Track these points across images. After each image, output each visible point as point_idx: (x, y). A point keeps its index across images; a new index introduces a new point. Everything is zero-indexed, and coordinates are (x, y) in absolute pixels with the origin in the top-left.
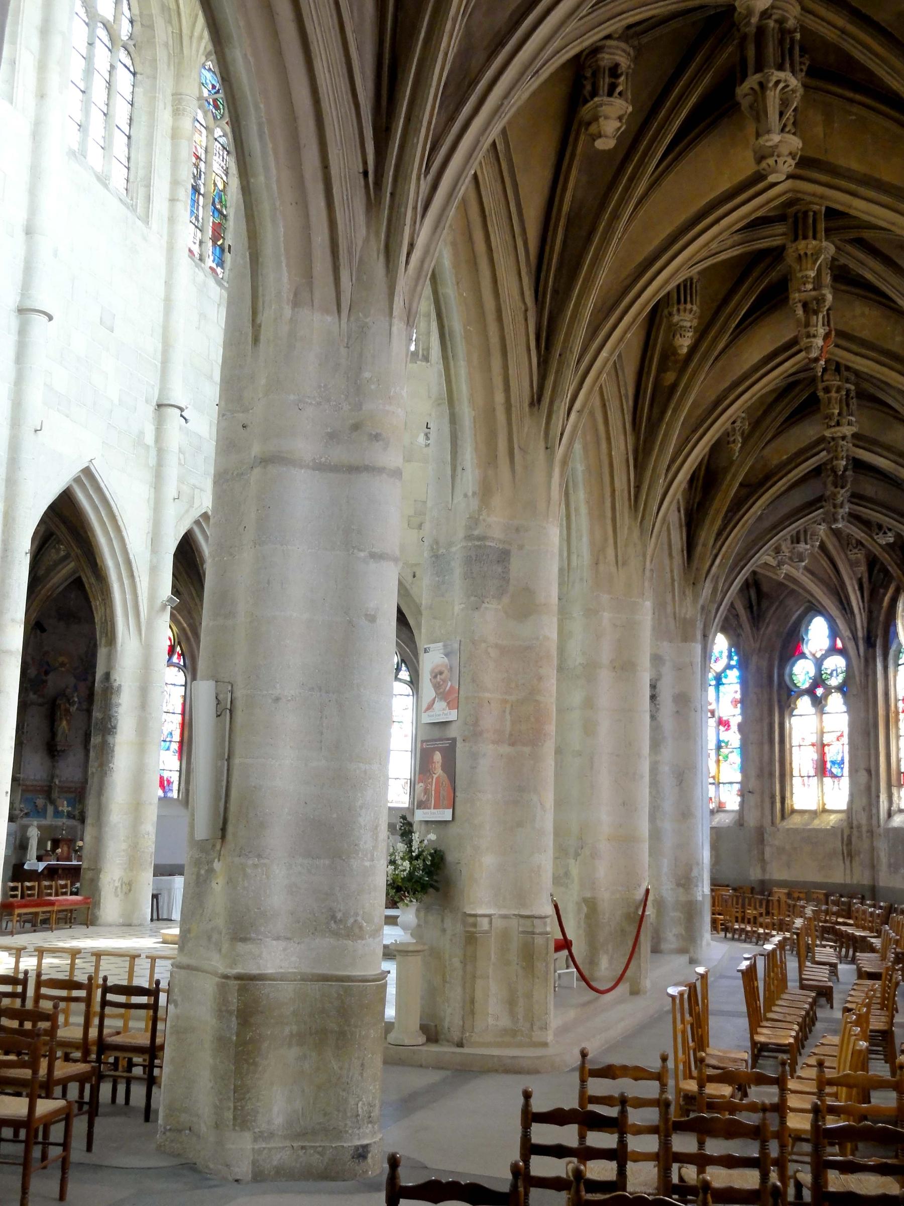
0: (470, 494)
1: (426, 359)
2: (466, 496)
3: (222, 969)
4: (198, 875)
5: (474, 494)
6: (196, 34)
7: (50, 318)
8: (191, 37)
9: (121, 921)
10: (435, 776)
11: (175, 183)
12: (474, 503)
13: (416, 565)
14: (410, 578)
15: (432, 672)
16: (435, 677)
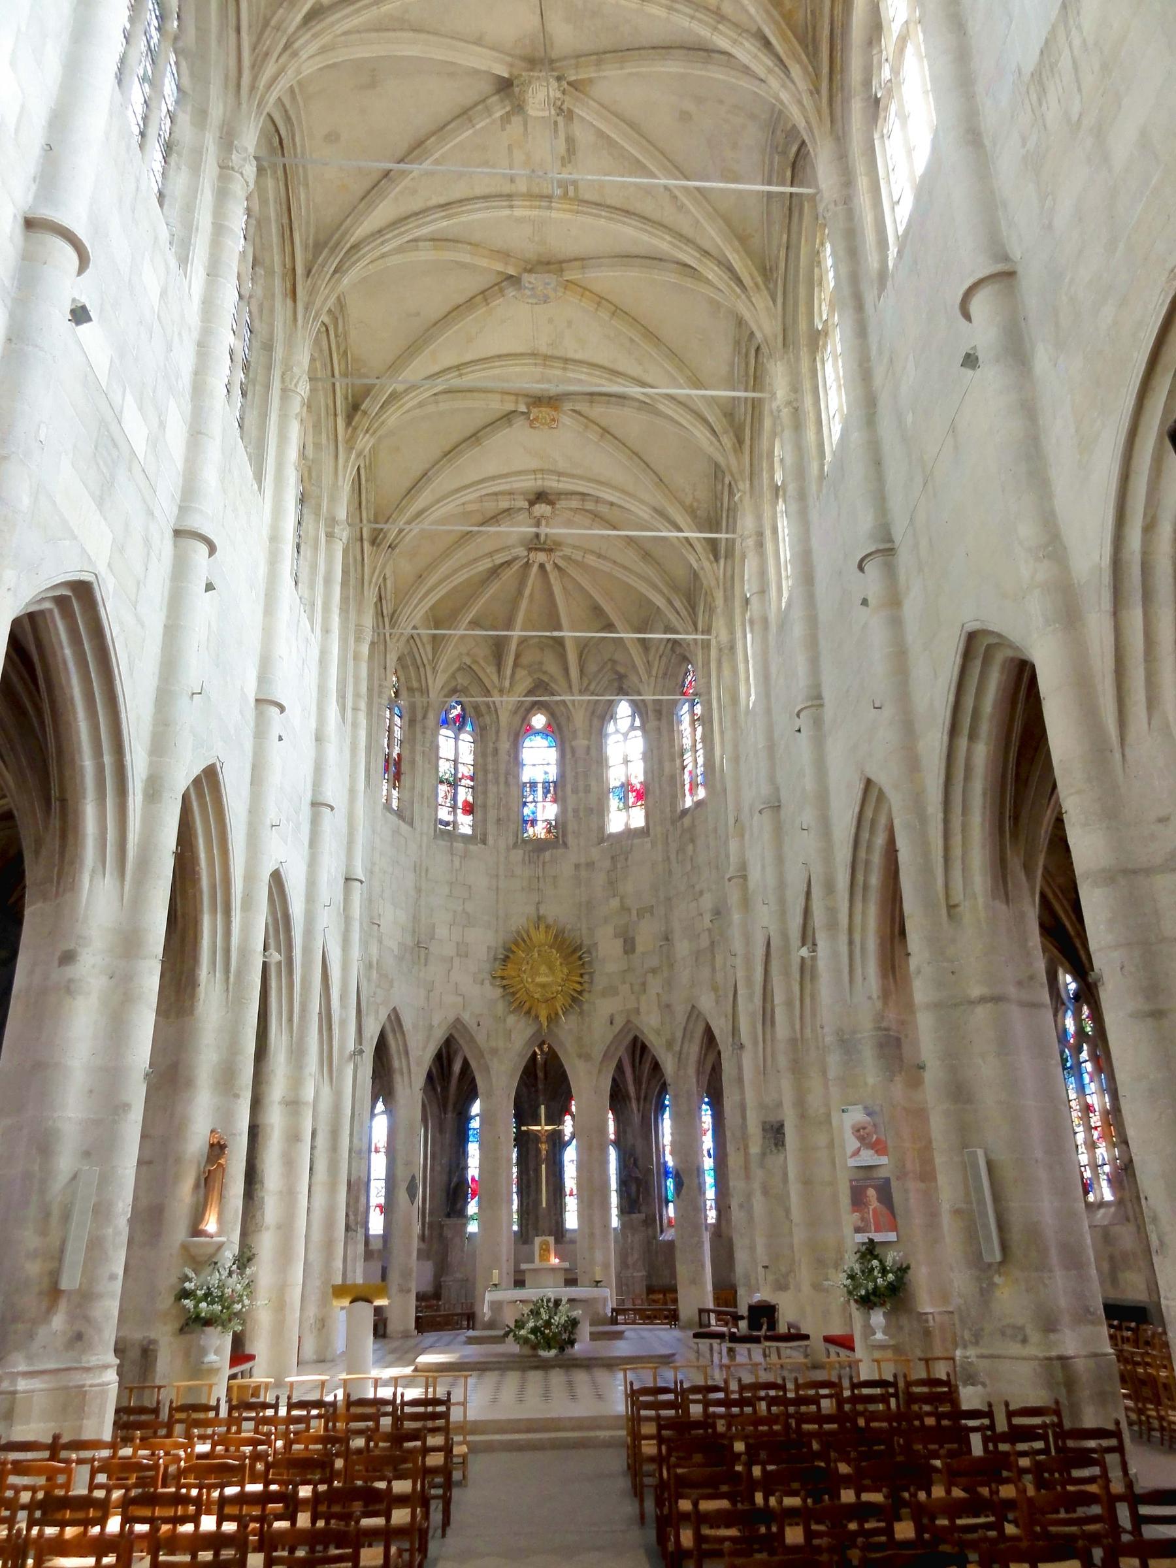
0: (875, 996)
1: (484, 842)
2: (870, 998)
3: (1041, 1355)
4: (981, 1289)
5: (879, 997)
6: (374, 580)
7: (332, 808)
8: (370, 583)
9: (315, 1357)
10: (871, 1208)
11: (357, 695)
12: (879, 1005)
13: (481, 1015)
14: (475, 1026)
15: (853, 1127)
16: (858, 1131)
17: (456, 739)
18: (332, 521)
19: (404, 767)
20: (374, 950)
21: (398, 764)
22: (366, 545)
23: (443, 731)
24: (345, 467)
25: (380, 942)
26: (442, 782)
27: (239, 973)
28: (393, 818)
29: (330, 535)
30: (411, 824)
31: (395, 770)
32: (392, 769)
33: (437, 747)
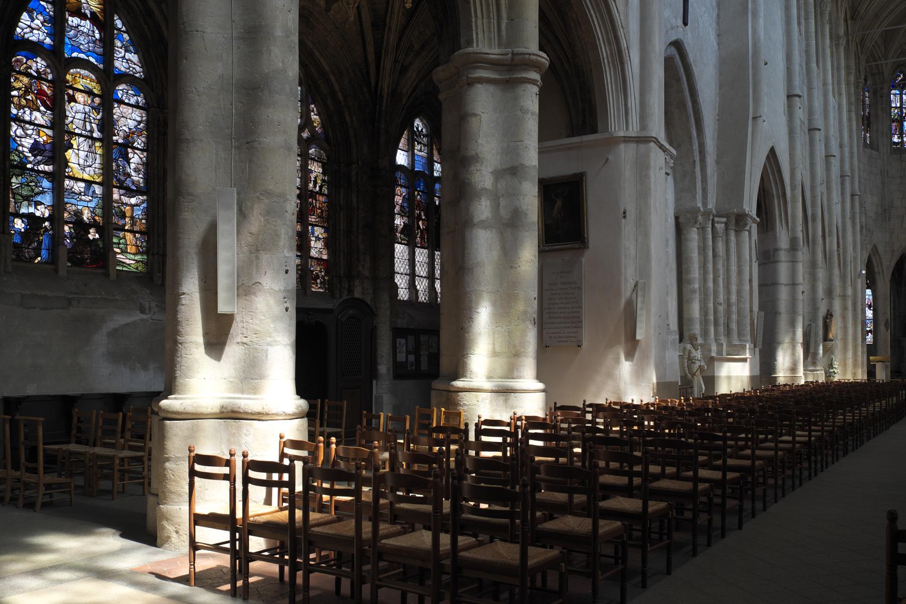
17: (901, 95)
18: (838, 37)
19: (872, 119)
20: (864, 220)
21: (868, 118)
22: (849, 22)
23: (893, 92)
24: (841, 6)
25: (866, 214)
26: (893, 121)
27: (830, 259)
28: (868, 150)
29: (837, 45)
30: (878, 150)
31: (867, 122)
32: (866, 122)
33: (890, 102)
